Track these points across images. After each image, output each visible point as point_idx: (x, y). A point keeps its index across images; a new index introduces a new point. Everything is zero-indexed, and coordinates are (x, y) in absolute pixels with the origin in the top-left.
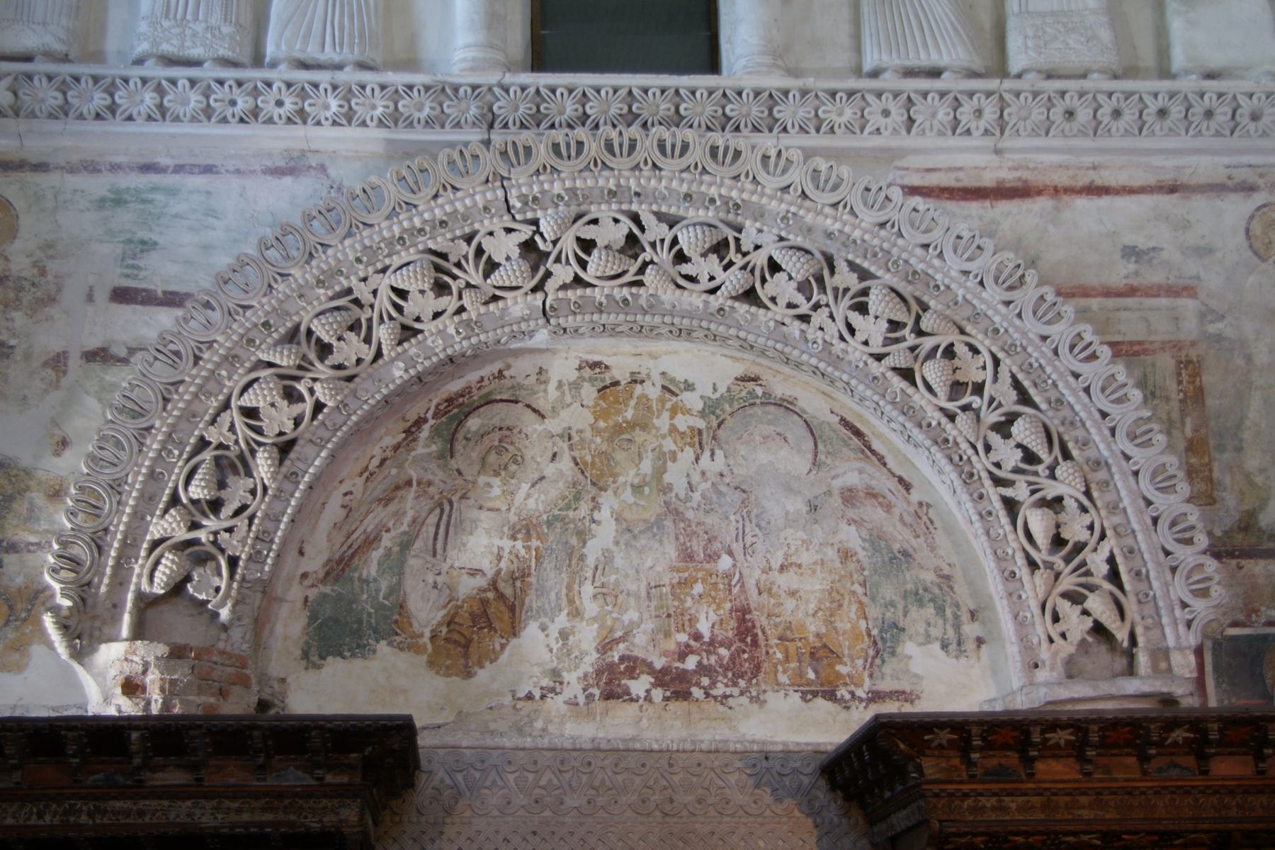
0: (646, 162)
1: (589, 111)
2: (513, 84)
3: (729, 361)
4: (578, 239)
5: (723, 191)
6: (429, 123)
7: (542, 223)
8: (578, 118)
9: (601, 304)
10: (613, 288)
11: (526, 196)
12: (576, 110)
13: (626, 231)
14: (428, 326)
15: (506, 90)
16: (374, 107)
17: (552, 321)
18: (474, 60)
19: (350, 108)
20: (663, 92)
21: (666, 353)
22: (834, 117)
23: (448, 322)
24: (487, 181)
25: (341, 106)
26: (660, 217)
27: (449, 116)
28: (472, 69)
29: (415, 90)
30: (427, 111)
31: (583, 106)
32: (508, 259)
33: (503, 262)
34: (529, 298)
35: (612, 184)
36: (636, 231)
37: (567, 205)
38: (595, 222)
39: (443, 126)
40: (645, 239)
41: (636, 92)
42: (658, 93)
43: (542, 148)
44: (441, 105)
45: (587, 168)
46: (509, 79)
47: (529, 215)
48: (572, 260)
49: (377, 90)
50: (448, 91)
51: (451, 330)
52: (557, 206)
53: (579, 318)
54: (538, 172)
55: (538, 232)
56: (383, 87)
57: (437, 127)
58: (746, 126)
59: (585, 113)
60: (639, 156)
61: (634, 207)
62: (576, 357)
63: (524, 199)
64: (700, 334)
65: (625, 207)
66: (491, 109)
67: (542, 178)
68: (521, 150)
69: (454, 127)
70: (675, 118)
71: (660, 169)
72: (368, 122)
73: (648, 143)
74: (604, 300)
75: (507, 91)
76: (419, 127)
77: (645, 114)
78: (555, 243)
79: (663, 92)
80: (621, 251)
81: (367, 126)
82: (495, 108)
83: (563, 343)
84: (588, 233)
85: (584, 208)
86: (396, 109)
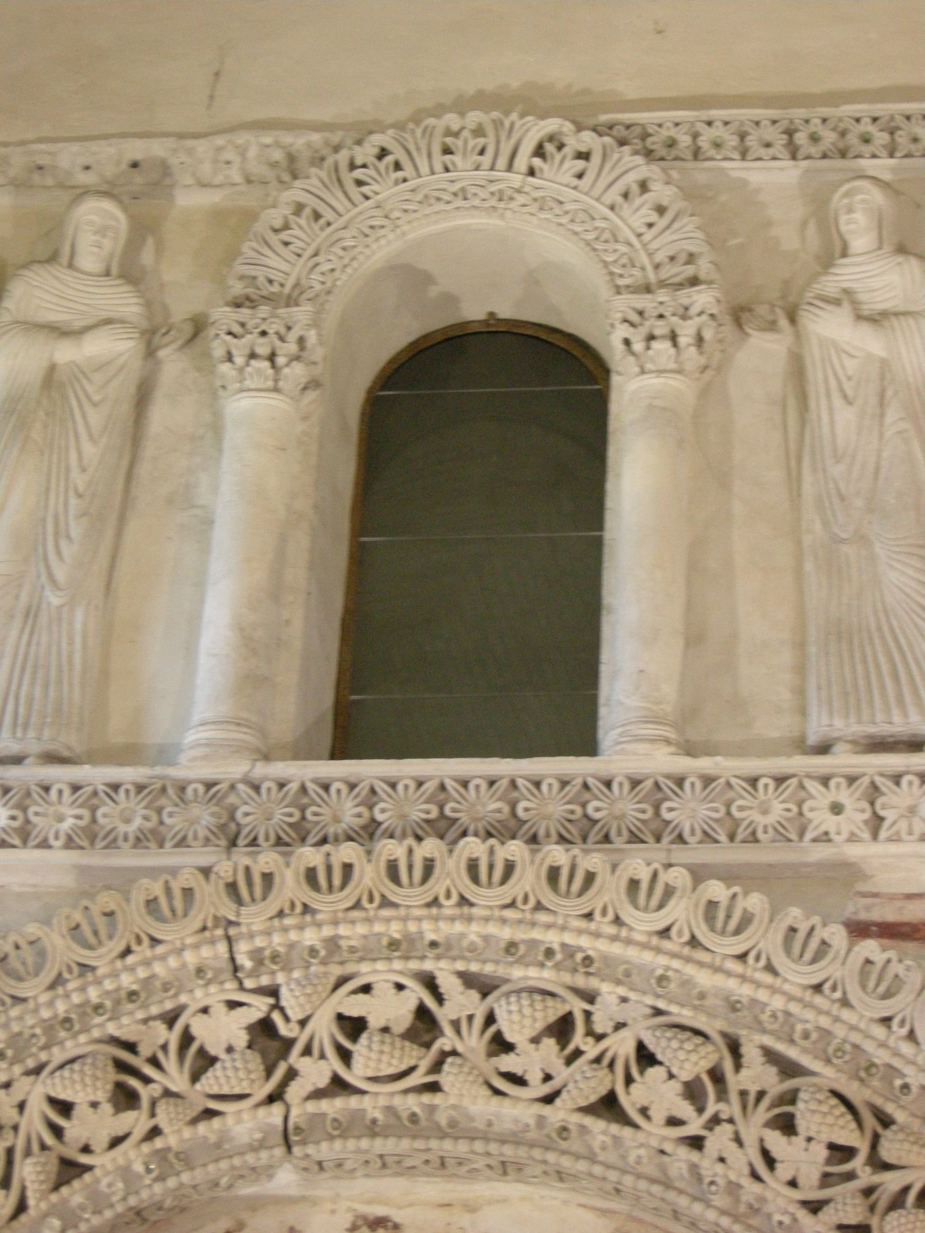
0: (448, 895)
1: (379, 817)
2: (266, 778)
3: (589, 1216)
4: (340, 1017)
5: (569, 939)
6: (139, 842)
7: (284, 992)
8: (364, 828)
9: (374, 1121)
10: (392, 1094)
11: (260, 950)
12: (359, 815)
13: (412, 1004)
14: (100, 1160)
15: (257, 788)
16: (61, 819)
17: (296, 1150)
18: (209, 744)
19: (27, 821)
20: (492, 783)
21: (490, 1202)
22: (761, 820)
23: (132, 1154)
24: (204, 929)
25: (13, 818)
26: (469, 980)
27: (171, 827)
28: (205, 757)
29: (122, 791)
30: (138, 822)
31: (371, 808)
32: (230, 1050)
33: (223, 1055)
34: (262, 1112)
35: (395, 930)
36: (430, 1003)
37: (324, 963)
38: (366, 989)
39: (161, 845)
40: (444, 1014)
41: (449, 784)
42: (484, 785)
43: (289, 874)
44: (159, 811)
45: (357, 905)
46: (261, 770)
47: (265, 981)
48: (330, 1052)
49: (67, 792)
50: (171, 791)
51: (139, 1167)
52: (308, 966)
53: (338, 1144)
54: (281, 914)
55: (277, 1006)
56: (76, 788)
57: (153, 845)
58: (619, 833)
59: (373, 820)
60: (437, 886)
61: (428, 966)
62: (349, 1209)
63: (257, 956)
64: (538, 1170)
65: (414, 965)
66: (232, 818)
67: (287, 921)
68: (257, 880)
69: (177, 845)
70: (512, 823)
71: (471, 905)
72: (52, 841)
73: (451, 863)
74: (378, 1114)
75: (257, 788)
76: (126, 846)
77: (464, 818)
78: (303, 1023)
79: (492, 783)
80: (410, 1035)
81: (49, 847)
82: (239, 815)
83: (325, 1187)
84: (355, 1007)
85: (350, 968)
86: (94, 820)
